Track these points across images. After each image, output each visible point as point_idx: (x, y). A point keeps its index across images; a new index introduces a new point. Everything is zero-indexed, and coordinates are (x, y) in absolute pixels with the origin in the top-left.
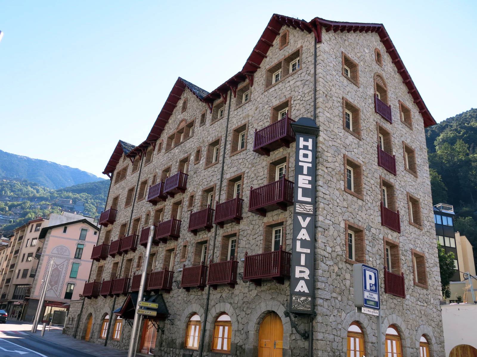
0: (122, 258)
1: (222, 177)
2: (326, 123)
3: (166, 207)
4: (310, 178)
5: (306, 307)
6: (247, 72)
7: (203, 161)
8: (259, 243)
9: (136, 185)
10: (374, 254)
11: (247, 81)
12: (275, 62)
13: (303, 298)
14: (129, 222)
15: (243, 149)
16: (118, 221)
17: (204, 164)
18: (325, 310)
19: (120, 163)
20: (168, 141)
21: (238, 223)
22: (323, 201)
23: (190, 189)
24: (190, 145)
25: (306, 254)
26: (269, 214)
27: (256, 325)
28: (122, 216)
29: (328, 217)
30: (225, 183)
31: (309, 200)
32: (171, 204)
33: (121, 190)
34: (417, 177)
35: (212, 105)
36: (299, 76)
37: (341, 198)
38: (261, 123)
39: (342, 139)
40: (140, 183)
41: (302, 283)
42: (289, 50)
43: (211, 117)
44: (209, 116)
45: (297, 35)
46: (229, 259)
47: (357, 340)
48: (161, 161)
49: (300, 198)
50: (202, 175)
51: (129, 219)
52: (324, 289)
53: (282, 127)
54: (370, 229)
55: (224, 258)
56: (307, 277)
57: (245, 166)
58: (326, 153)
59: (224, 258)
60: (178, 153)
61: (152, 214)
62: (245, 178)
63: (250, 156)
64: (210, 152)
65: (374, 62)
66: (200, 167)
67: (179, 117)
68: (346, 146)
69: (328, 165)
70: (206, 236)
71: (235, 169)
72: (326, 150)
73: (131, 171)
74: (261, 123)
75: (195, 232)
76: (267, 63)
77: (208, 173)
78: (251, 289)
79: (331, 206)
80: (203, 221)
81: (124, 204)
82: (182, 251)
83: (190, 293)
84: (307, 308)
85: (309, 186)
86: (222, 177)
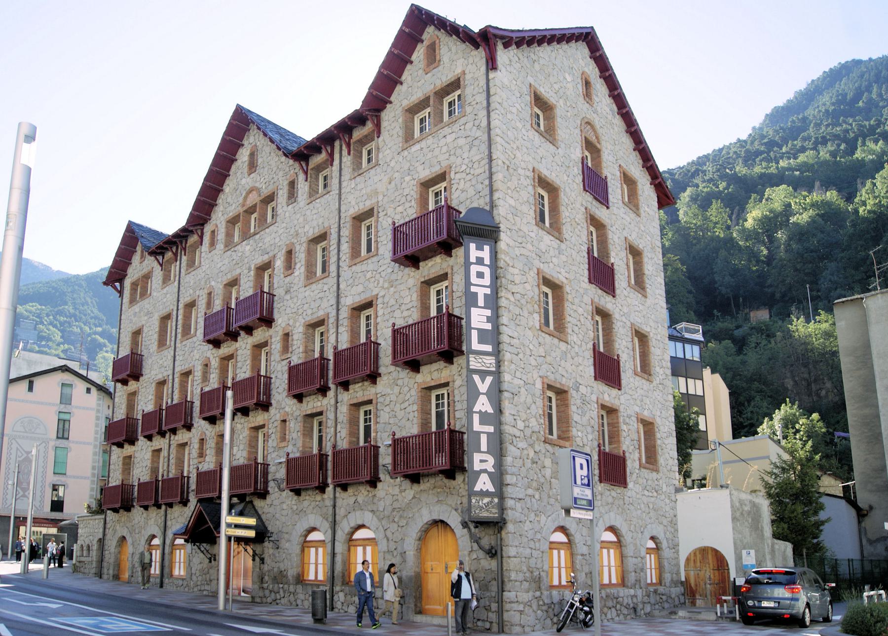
0: (167, 441)
1: (338, 303)
2: (510, 216)
3: (239, 352)
4: (488, 312)
5: (491, 512)
6: (369, 110)
7: (300, 270)
8: (411, 416)
9: (175, 308)
10: (585, 432)
11: (369, 125)
12: (417, 96)
13: (486, 500)
14: (171, 377)
15: (371, 254)
16: (149, 376)
17: (303, 277)
18: (518, 515)
19: (134, 264)
20: (227, 227)
21: (374, 382)
22: (510, 349)
23: (281, 320)
24: (272, 240)
25: (488, 434)
26: (424, 369)
27: (417, 542)
28: (155, 367)
29: (518, 374)
30: (345, 313)
31: (488, 348)
32: (249, 347)
33: (146, 318)
34: (646, 297)
35: (307, 165)
36: (462, 128)
37: (535, 342)
38: (400, 209)
39: (535, 243)
40: (181, 306)
41: (484, 478)
42: (442, 76)
43: (307, 188)
44: (303, 187)
45: (454, 49)
46: (362, 443)
47: (562, 552)
48: (219, 266)
49: (476, 345)
50: (301, 296)
51: (170, 372)
52: (515, 485)
53: (439, 220)
54: (578, 388)
55: (354, 439)
57: (378, 284)
58: (511, 270)
59: (354, 439)
60: (249, 254)
61: (215, 363)
62: (380, 306)
63: (385, 267)
64: (310, 254)
65: (581, 99)
66: (296, 281)
67: (244, 181)
68: (541, 254)
69: (515, 289)
70: (319, 404)
71: (360, 288)
72: (511, 264)
73: (160, 282)
74: (400, 209)
75: (299, 398)
76: (404, 95)
78: (403, 488)
79: (521, 356)
80: (308, 380)
81: (156, 343)
82: (278, 429)
83: (301, 498)
84: (491, 514)
85: (488, 326)
86: (338, 303)
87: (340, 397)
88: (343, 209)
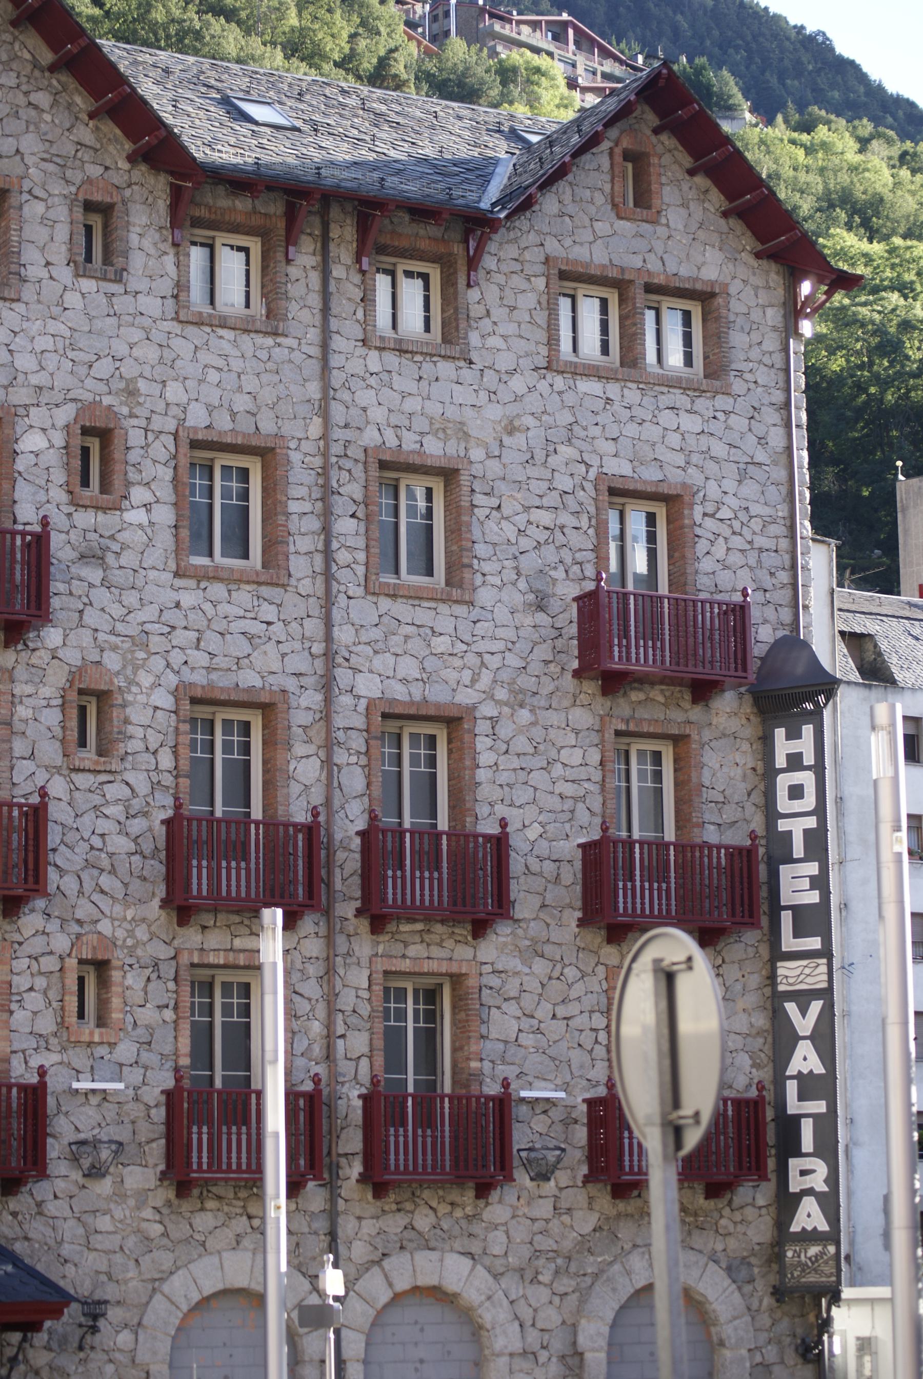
13: (813, 1250)
30: (349, 715)
56: (821, 1187)
71: (409, 668)
77: (207, 607)
78: (564, 1205)
88: (338, 412)
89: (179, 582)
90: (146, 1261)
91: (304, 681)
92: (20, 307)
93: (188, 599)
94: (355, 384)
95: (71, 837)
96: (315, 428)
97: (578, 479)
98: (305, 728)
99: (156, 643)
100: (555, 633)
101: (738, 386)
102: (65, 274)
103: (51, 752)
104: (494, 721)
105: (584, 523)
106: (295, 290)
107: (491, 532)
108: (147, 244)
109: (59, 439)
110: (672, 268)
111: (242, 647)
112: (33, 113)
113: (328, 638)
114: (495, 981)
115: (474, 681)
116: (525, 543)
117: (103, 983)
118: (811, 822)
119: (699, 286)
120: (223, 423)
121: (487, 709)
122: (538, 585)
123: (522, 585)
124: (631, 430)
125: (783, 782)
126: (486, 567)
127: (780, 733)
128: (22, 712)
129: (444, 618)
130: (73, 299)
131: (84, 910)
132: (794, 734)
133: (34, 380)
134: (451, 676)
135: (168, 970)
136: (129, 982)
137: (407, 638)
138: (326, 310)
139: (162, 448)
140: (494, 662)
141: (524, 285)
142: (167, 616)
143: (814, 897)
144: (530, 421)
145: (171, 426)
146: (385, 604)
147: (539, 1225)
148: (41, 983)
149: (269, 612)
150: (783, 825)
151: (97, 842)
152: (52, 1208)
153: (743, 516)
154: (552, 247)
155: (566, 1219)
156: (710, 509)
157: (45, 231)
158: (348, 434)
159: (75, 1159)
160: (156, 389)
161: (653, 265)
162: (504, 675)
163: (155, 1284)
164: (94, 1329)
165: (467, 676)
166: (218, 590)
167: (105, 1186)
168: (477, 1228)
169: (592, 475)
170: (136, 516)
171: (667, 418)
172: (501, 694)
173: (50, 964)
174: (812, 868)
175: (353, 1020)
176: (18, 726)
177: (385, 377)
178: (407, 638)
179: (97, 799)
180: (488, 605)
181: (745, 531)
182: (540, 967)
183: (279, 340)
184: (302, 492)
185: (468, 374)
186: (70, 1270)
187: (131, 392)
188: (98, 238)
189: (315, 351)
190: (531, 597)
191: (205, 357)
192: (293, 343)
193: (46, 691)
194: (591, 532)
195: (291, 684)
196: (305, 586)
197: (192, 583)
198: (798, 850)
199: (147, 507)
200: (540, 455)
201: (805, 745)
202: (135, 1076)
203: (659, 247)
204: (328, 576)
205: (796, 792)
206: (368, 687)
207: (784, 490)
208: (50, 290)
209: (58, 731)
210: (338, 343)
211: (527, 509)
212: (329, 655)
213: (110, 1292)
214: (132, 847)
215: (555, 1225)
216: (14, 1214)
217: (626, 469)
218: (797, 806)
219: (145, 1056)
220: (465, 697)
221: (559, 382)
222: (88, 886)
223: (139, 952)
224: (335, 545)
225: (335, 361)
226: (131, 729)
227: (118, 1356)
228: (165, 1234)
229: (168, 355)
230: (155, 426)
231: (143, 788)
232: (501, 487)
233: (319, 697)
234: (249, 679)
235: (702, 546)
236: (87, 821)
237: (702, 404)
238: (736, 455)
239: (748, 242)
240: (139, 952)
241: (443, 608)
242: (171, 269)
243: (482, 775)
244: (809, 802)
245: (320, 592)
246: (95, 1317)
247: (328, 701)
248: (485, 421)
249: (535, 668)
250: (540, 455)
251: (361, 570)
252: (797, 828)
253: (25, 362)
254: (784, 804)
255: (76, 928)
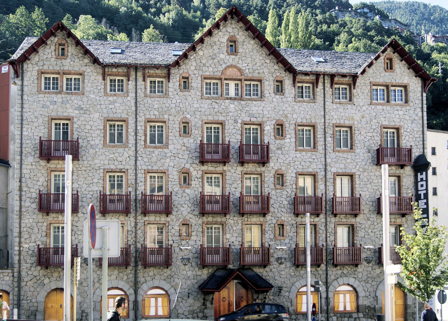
23: (274, 165)
33: (78, 112)
71: (342, 166)
77: (302, 157)
87: (328, 219)
88: (327, 117)
89: (296, 152)
90: (291, 280)
91: (321, 170)
92: (264, 102)
93: (298, 155)
94: (331, 111)
95: (276, 202)
96: (323, 121)
97: (377, 126)
98: (321, 179)
99: (292, 164)
100: (372, 157)
101: (411, 104)
102: (273, 95)
103: (272, 186)
104: (359, 175)
105: (378, 135)
106: (318, 94)
107: (358, 138)
108: (289, 87)
109: (272, 127)
110: (397, 82)
111: (308, 164)
112: (266, 64)
113: (325, 161)
114: (360, 225)
115: (355, 168)
116: (366, 140)
117: (283, 228)
118: (425, 192)
119: (403, 85)
120: (304, 121)
121: (358, 173)
122: (368, 148)
123: (365, 148)
124: (388, 115)
125: (420, 184)
126: (358, 145)
127: (419, 174)
128: (266, 179)
129: (349, 155)
130: (275, 100)
131: (279, 215)
132: (422, 174)
133: (267, 116)
134: (351, 167)
135: (295, 226)
136: (287, 228)
137: (342, 160)
138: (324, 97)
139: (293, 127)
140: (359, 164)
141: (366, 88)
142: (294, 159)
143: (425, 207)
144: (367, 115)
145: (294, 122)
146: (337, 153)
147: (368, 272)
148: (271, 229)
149: (314, 157)
150: (419, 192)
151: (281, 202)
152: (273, 270)
153: (412, 131)
154: (372, 80)
155: (374, 271)
156: (405, 130)
157: (269, 87)
158: (330, 121)
159: (277, 261)
160: (291, 115)
161: (393, 81)
162: (361, 166)
163: (293, 284)
164: (280, 292)
165: (354, 167)
166: (304, 153)
167: (283, 266)
168: (356, 273)
169: (380, 125)
170: (288, 140)
171: (396, 112)
172: (361, 170)
173: (273, 225)
174: (425, 201)
175: (331, 234)
176: (266, 182)
177: (337, 109)
178: (342, 160)
179: (281, 194)
180: (358, 153)
181: (413, 134)
182: (369, 222)
183: (316, 104)
184: (321, 133)
185: (354, 107)
186: (277, 282)
187: (286, 117)
188: (279, 88)
189: (323, 105)
190: (367, 150)
191: (301, 109)
192: (318, 104)
193: (271, 175)
194: (380, 136)
195: (319, 171)
196: (321, 152)
197: (299, 152)
198: (422, 197)
199: (290, 138)
200: (369, 122)
201: (424, 176)
202: (289, 245)
203: (394, 77)
204: (325, 149)
205: (422, 186)
206: (334, 170)
207: (421, 125)
208: (270, 98)
209: (273, 182)
210: (327, 103)
211: (366, 133)
212: (326, 165)
213: (284, 285)
214: (288, 203)
215: (372, 272)
216: (266, 271)
217: (387, 123)
218: (422, 188)
219: (291, 242)
220: (353, 171)
221: (373, 107)
222: (279, 211)
223: (289, 222)
224: (327, 143)
225: (326, 107)
226: (287, 181)
227: (286, 297)
228: (295, 275)
229: (293, 109)
230: (291, 123)
231: (290, 192)
232: (361, 129)
233: (324, 173)
234: (310, 170)
235: (403, 138)
236: (279, 199)
237: (403, 109)
238: (411, 118)
239: (414, 74)
240: (289, 222)
241: (349, 154)
242: (294, 92)
243: (357, 186)
244: (424, 188)
245: (324, 152)
246: (280, 290)
247: (326, 173)
248: (357, 117)
249: (368, 164)
250: (369, 122)
251: (332, 148)
252: (422, 193)
253: (266, 113)
254: (420, 188)
255: (277, 219)
